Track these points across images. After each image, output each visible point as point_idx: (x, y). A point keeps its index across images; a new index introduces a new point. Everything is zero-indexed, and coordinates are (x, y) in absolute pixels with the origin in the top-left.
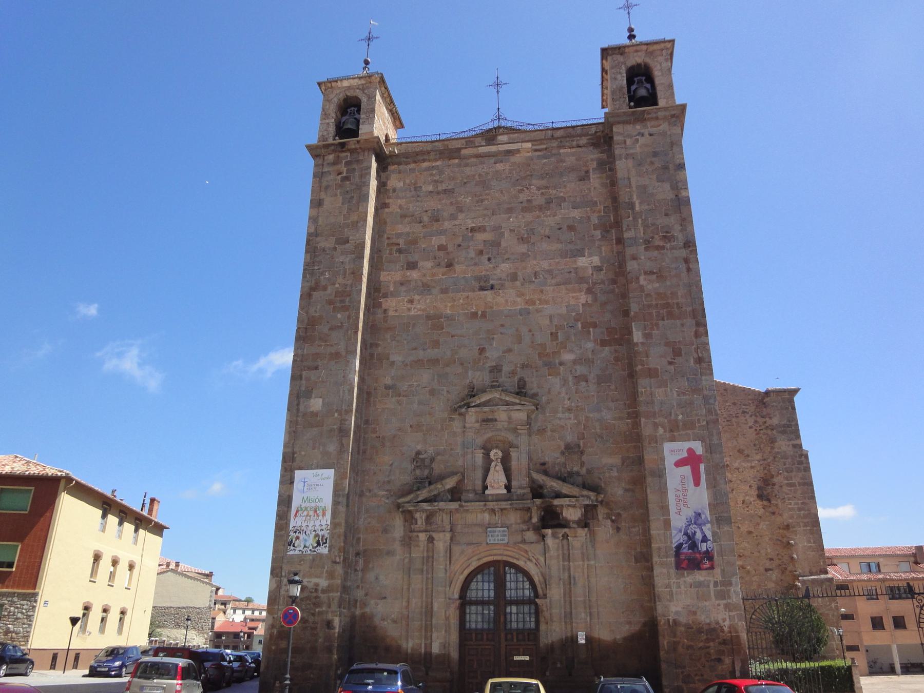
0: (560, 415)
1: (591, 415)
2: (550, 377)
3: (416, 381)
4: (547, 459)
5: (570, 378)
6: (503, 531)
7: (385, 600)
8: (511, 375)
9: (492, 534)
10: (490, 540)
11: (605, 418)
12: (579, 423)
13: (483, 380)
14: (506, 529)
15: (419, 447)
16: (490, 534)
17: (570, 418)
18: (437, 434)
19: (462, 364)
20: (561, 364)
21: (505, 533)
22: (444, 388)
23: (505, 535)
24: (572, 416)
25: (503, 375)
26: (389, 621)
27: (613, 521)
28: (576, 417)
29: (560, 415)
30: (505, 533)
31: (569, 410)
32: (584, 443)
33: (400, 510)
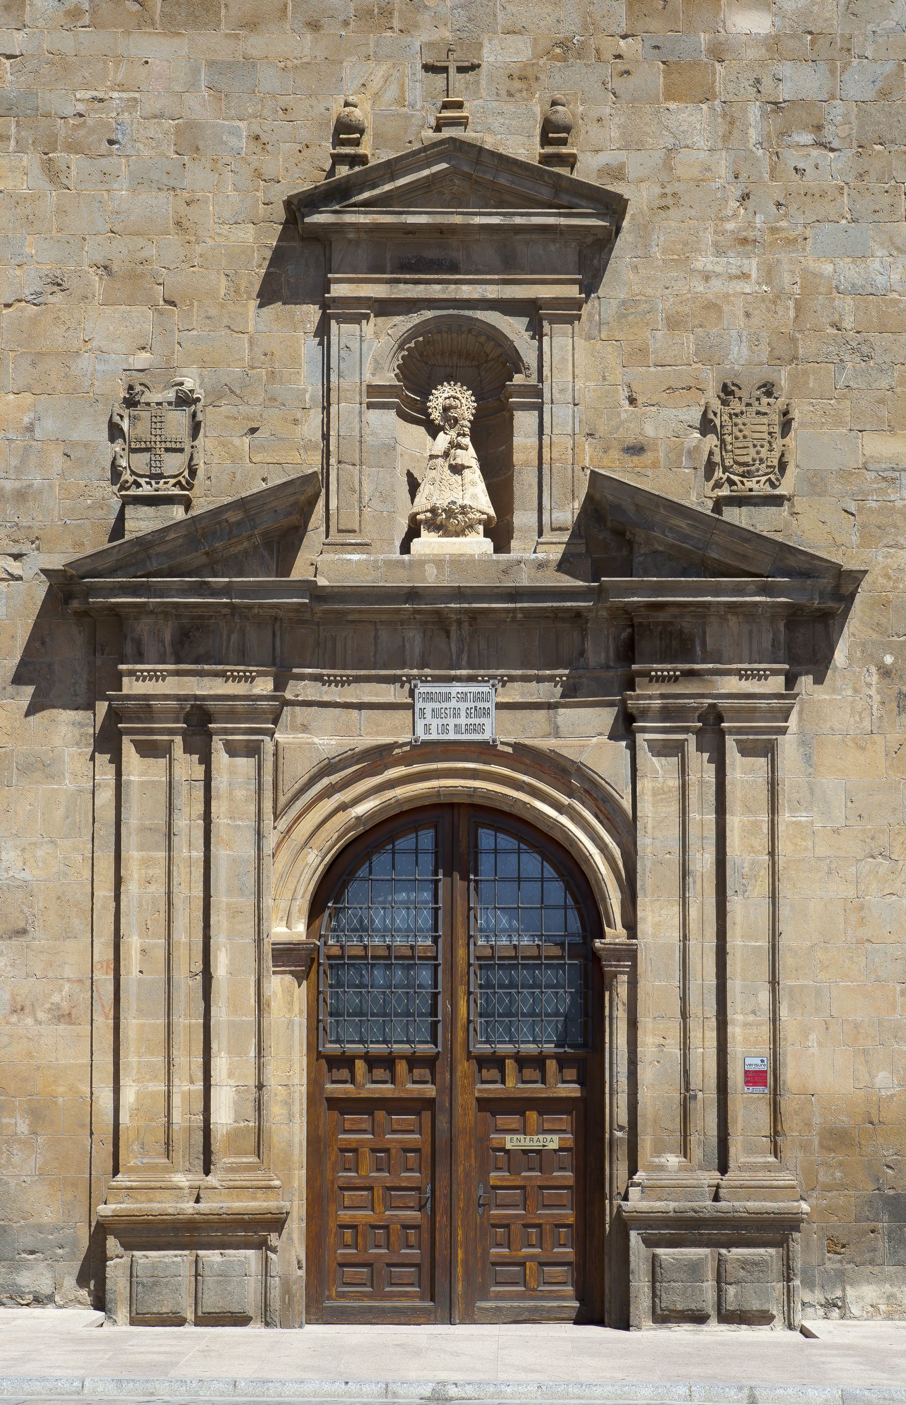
0: (704, 261)
1: (828, 268)
2: (672, 105)
3: (121, 87)
4: (650, 431)
5: (754, 112)
6: (478, 697)
7: (22, 940)
8: (517, 84)
9: (436, 705)
10: (427, 728)
11: (880, 280)
12: (778, 297)
13: (401, 101)
14: (485, 689)
15: (142, 359)
16: (429, 706)
17: (745, 276)
18: (213, 312)
19: (314, 26)
20: (718, 53)
21: (481, 705)
22: (242, 125)
23: (486, 713)
24: (752, 266)
25: (483, 83)
26: (41, 1015)
27: (885, 672)
28: (769, 273)
29: (704, 261)
30: (481, 705)
31: (745, 241)
32: (793, 378)
33: (75, 604)
